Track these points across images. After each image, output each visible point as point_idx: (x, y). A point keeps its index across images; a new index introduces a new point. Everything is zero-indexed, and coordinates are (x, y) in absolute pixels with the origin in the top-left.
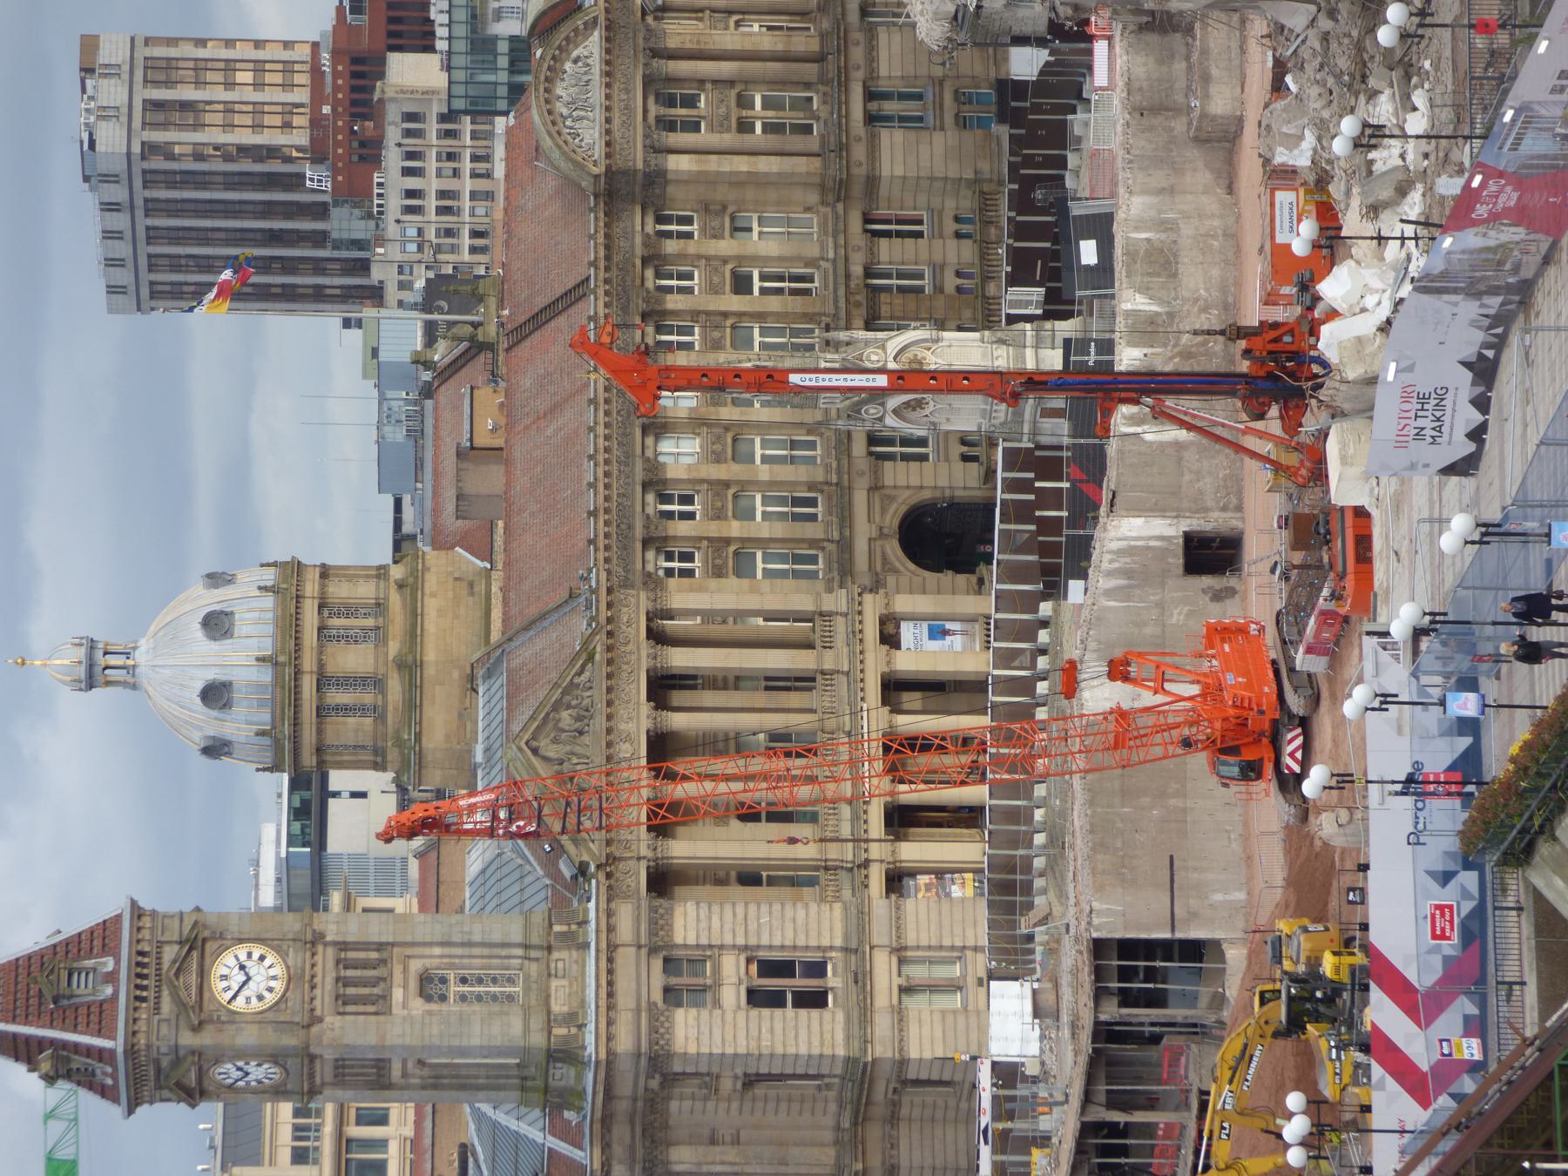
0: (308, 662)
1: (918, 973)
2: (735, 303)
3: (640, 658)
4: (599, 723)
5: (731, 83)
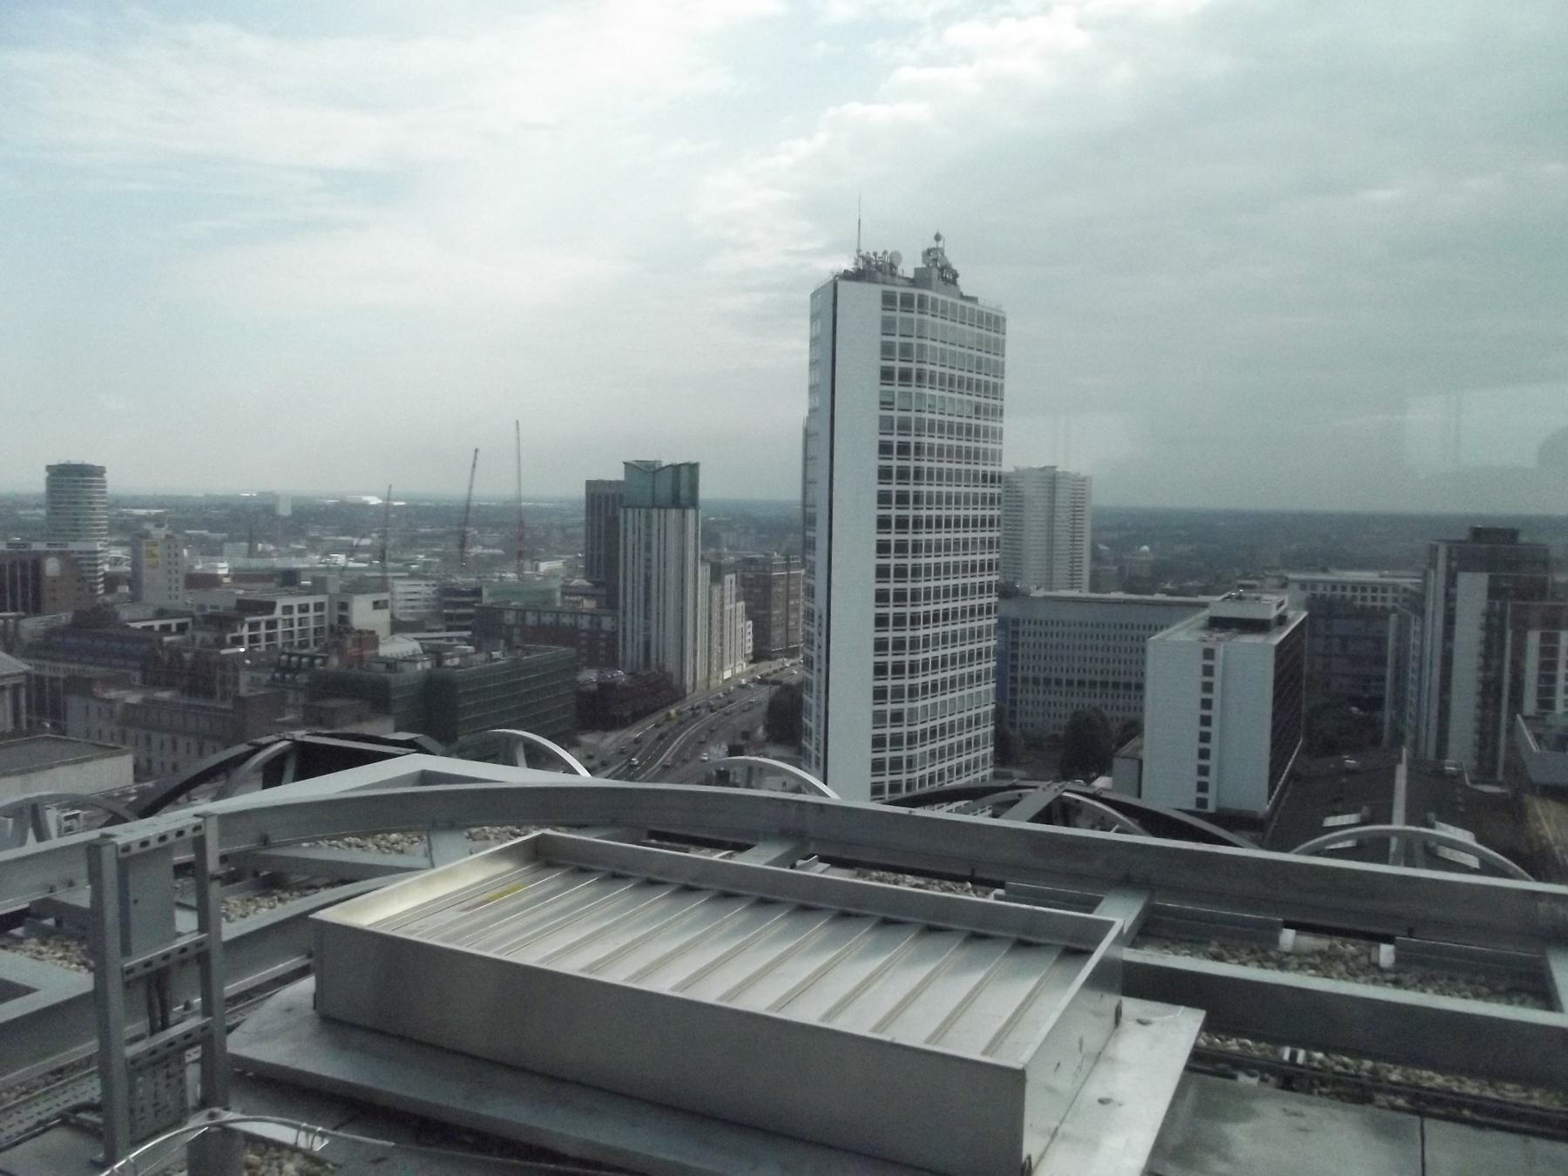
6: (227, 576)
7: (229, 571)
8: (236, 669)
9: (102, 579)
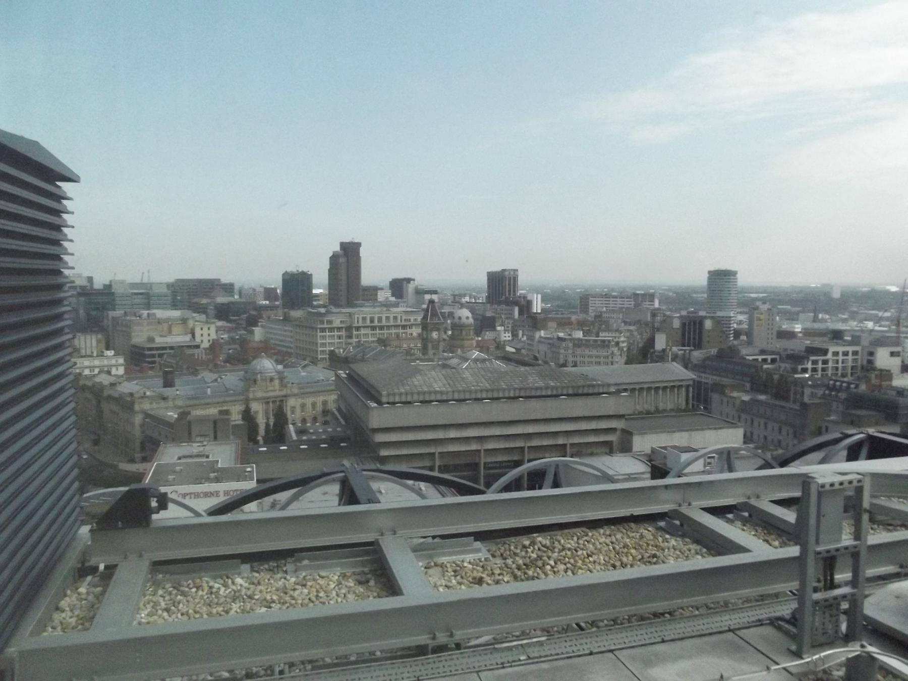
6: (800, 332)
7: (802, 329)
8: (803, 387)
9: (732, 332)
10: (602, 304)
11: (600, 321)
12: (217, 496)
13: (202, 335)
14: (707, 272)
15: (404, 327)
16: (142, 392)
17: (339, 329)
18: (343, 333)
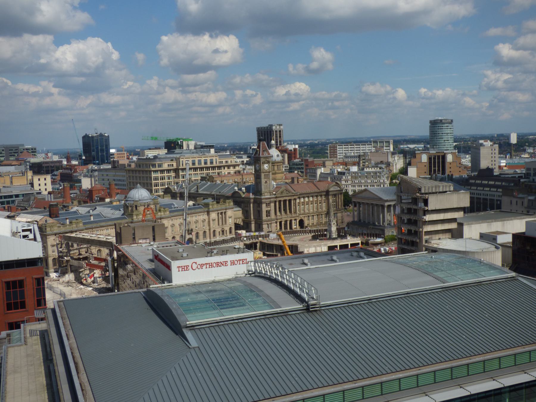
0: (275, 164)
1: (269, 225)
2: (319, 203)
3: (293, 198)
4: (287, 195)
5: (336, 201)
10: (348, 150)
11: (364, 159)
12: (225, 266)
13: (39, 185)
14: (429, 122)
15: (219, 167)
16: (44, 220)
17: (168, 171)
18: (173, 174)
